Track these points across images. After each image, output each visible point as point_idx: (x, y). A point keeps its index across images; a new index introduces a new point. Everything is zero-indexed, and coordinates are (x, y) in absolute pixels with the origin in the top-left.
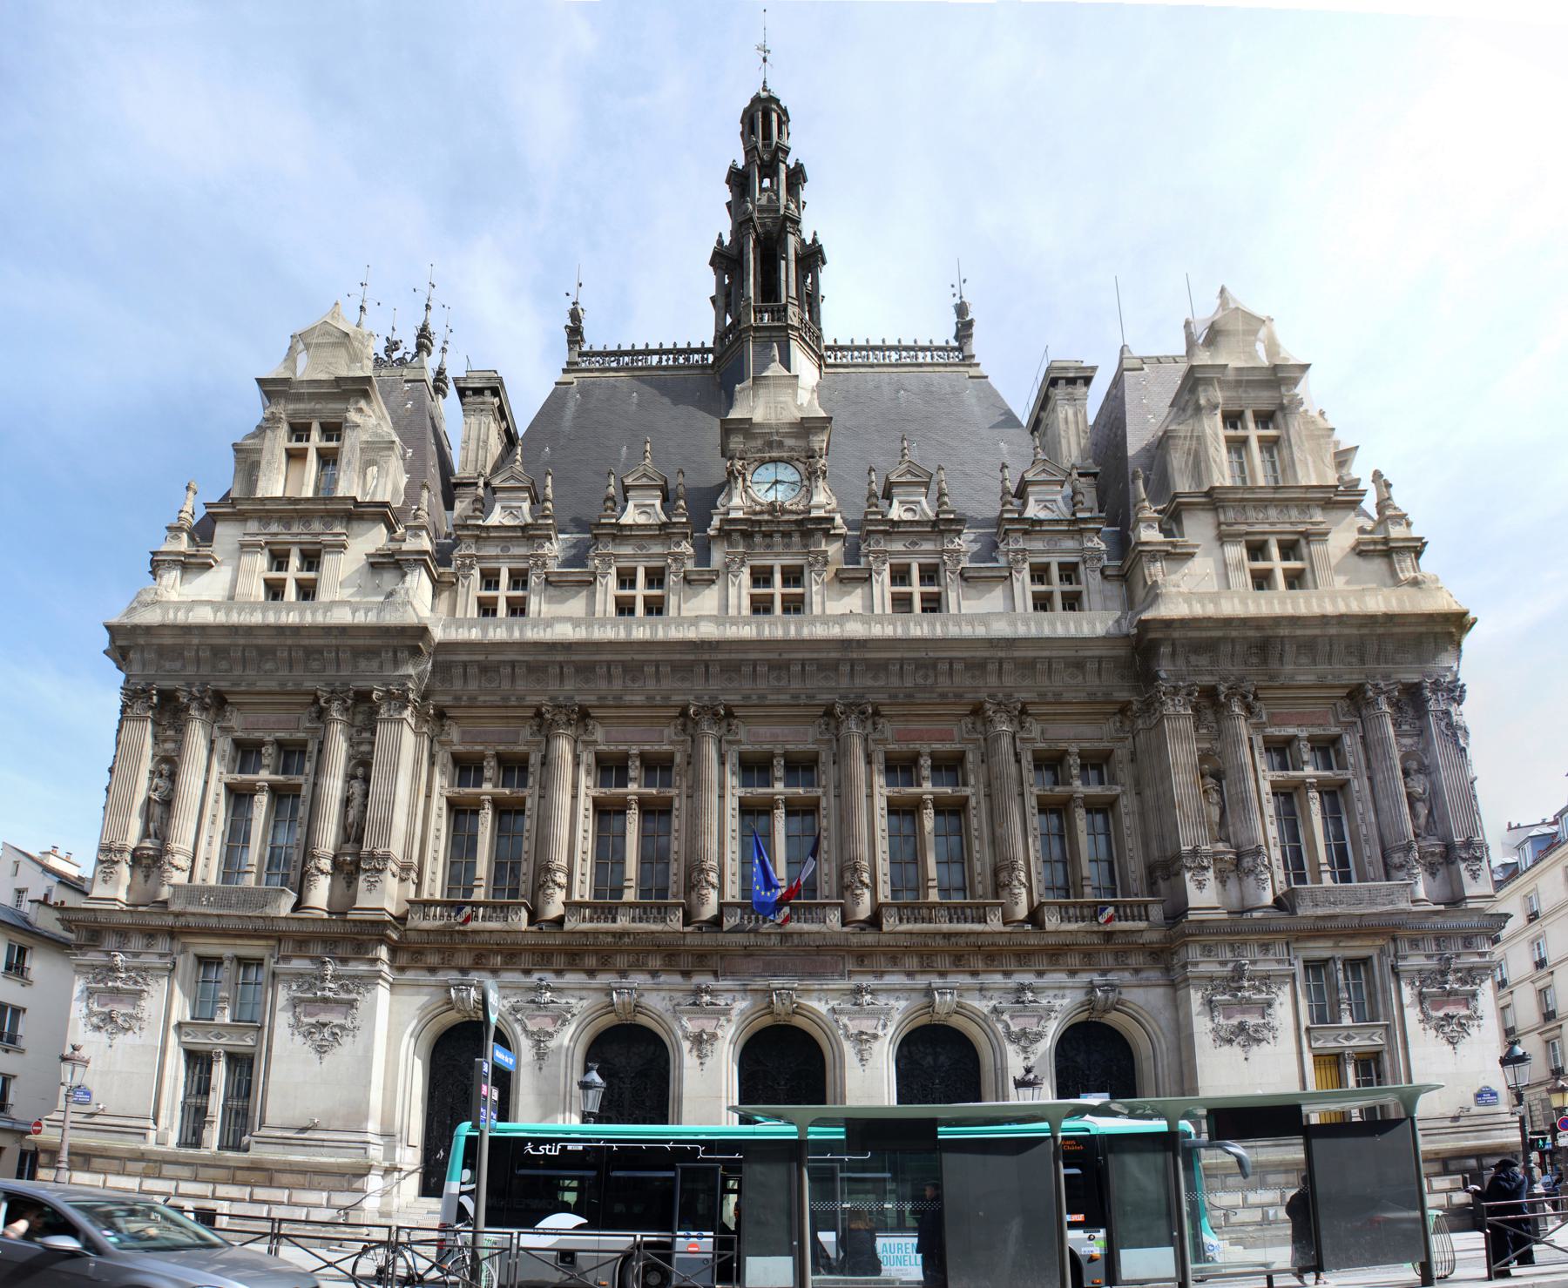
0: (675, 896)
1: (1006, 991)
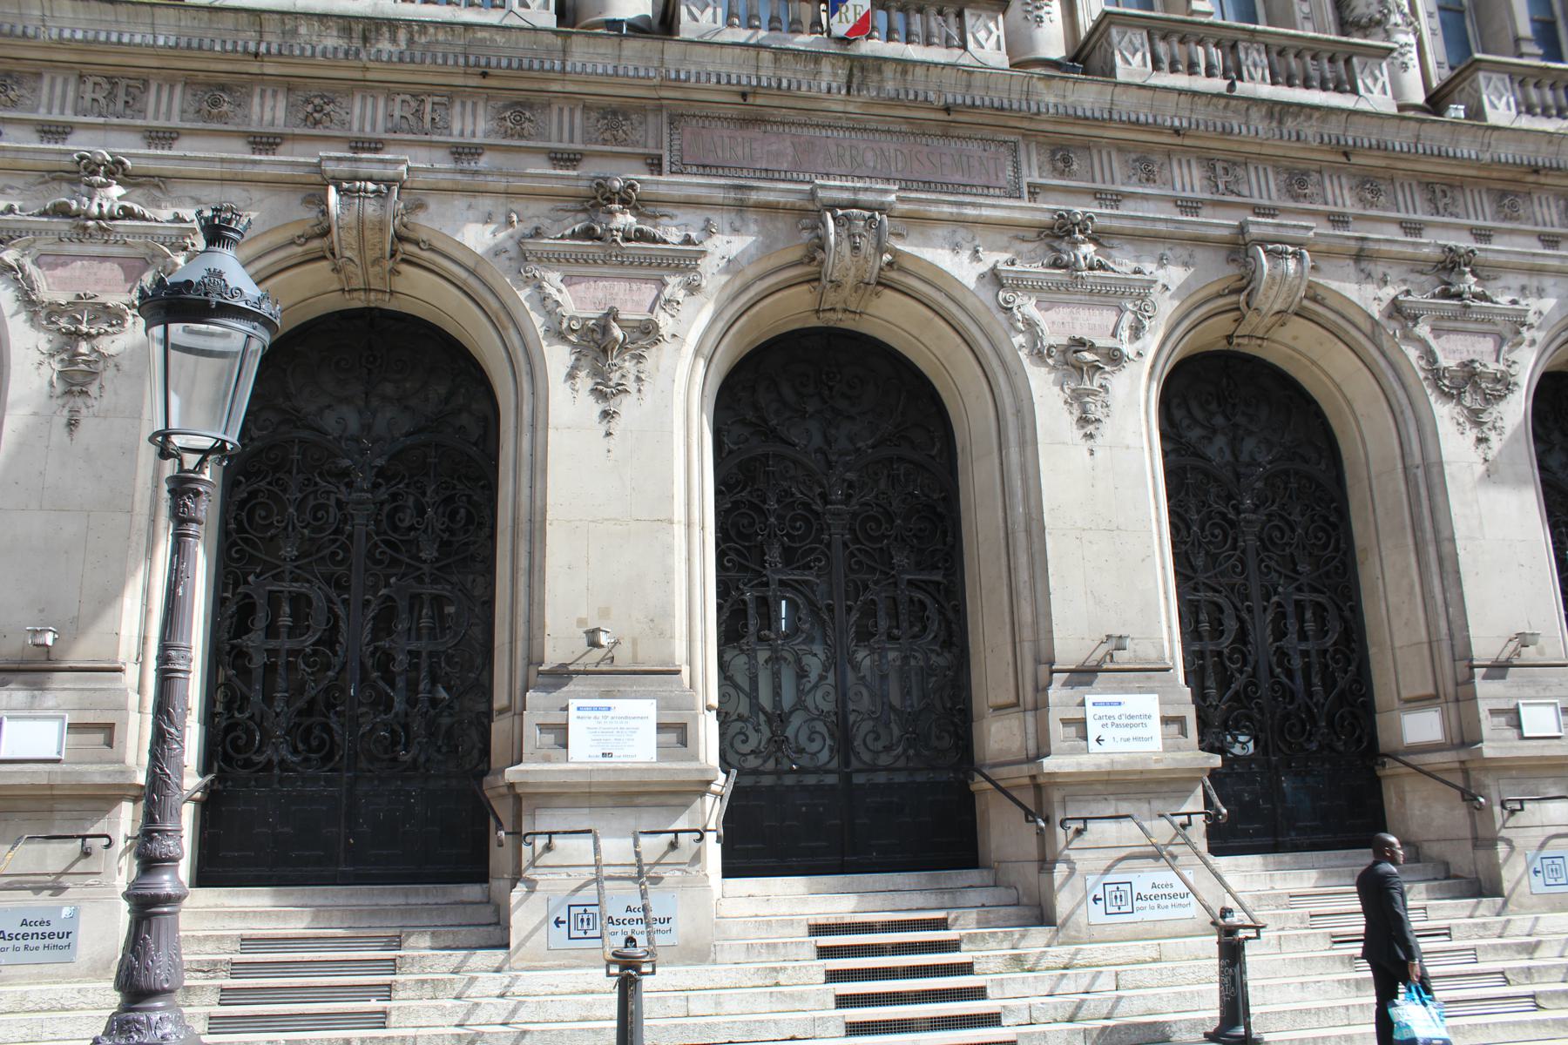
1: (1416, 265)
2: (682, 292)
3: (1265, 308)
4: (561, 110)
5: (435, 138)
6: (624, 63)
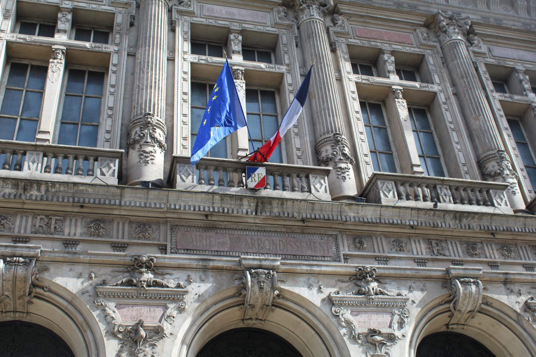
2: (176, 312)
3: (463, 310)
4: (118, 223)
5: (56, 236)
6: (149, 201)
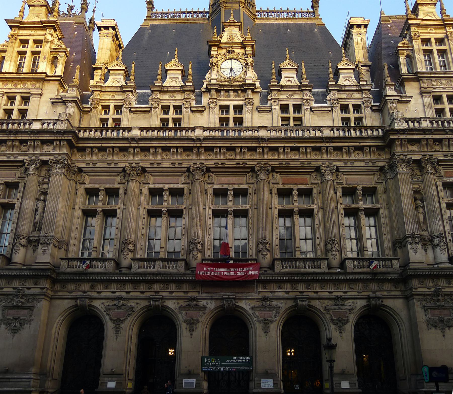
0: (182, 256)
